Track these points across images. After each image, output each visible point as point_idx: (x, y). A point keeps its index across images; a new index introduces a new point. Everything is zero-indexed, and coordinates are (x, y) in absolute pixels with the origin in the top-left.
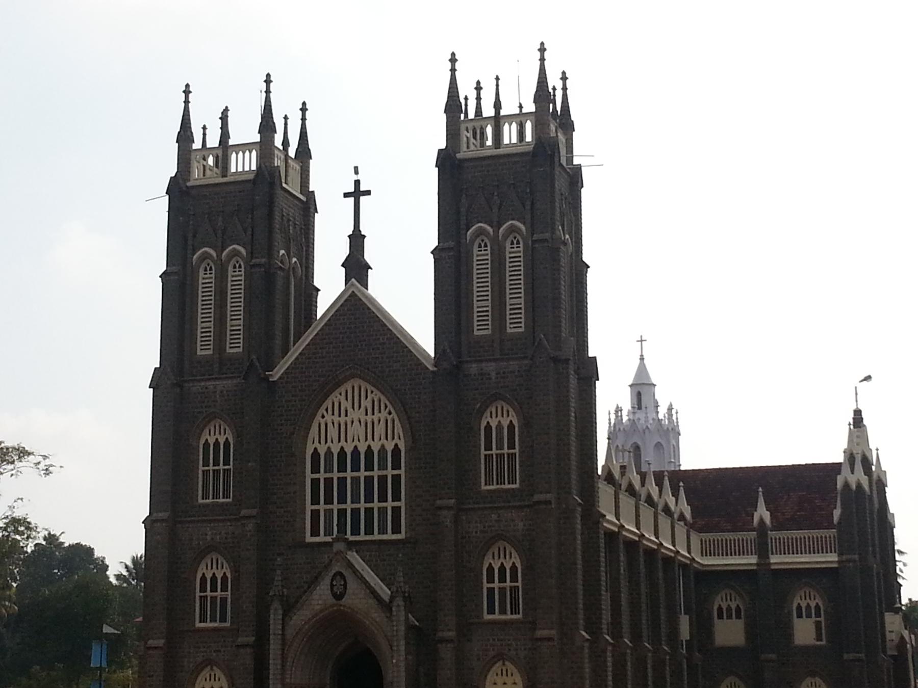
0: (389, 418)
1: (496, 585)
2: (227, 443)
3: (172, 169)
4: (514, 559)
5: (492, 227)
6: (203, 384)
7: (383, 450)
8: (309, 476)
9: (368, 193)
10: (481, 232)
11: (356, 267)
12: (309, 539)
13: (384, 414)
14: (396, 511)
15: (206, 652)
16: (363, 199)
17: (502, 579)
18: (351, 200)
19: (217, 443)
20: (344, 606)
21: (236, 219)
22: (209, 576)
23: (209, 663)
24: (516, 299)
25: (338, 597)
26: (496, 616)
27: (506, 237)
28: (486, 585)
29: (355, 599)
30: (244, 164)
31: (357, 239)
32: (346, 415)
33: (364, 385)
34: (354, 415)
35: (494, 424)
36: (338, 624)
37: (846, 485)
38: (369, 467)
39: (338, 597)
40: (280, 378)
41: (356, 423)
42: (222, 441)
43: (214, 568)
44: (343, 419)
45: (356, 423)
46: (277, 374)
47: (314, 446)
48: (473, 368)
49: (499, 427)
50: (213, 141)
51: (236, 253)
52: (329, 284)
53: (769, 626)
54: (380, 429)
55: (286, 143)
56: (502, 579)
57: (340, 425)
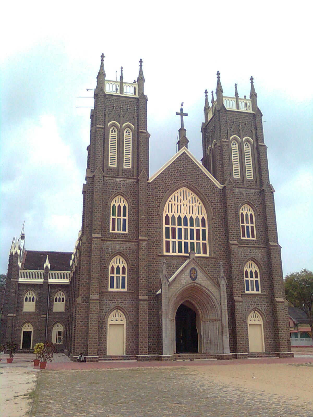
0: (200, 205)
2: (125, 207)
4: (255, 269)
5: (240, 137)
6: (114, 179)
12: (165, 253)
13: (197, 204)
14: (204, 245)
15: (115, 303)
19: (119, 206)
20: (197, 283)
22: (115, 267)
23: (117, 308)
24: (249, 166)
25: (194, 279)
27: (245, 142)
28: (245, 279)
32: (180, 202)
33: (188, 191)
34: (186, 202)
39: (194, 279)
40: (152, 182)
41: (184, 206)
42: (122, 206)
43: (118, 262)
45: (185, 206)
47: (166, 213)
51: (128, 127)
54: (195, 210)
57: (177, 206)
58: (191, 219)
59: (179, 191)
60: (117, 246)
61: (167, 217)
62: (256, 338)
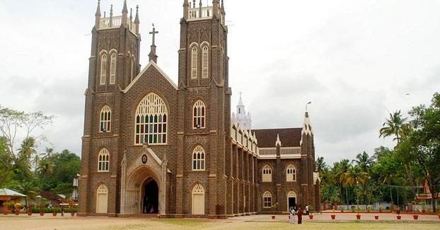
1: (197, 160)
2: (109, 113)
3: (94, 25)
4: (202, 151)
7: (160, 116)
8: (136, 124)
9: (157, 32)
10: (194, 45)
11: (153, 56)
12: (136, 144)
13: (161, 104)
16: (156, 34)
17: (199, 158)
18: (152, 35)
19: (106, 113)
21: (115, 42)
24: (205, 67)
26: (197, 170)
28: (193, 160)
29: (149, 164)
30: (117, 24)
31: (153, 47)
33: (155, 95)
34: (152, 104)
35: (197, 107)
36: (144, 171)
37: (304, 133)
38: (156, 121)
41: (152, 106)
44: (147, 106)
46: (125, 91)
48: (191, 89)
49: (199, 109)
50: (108, 15)
51: (114, 52)
52: (144, 62)
53: (279, 177)
54: (160, 109)
55: (131, 17)
56: (199, 158)
58: (156, 116)
59: (147, 96)
60: (103, 142)
61: (138, 117)
62: (198, 205)
